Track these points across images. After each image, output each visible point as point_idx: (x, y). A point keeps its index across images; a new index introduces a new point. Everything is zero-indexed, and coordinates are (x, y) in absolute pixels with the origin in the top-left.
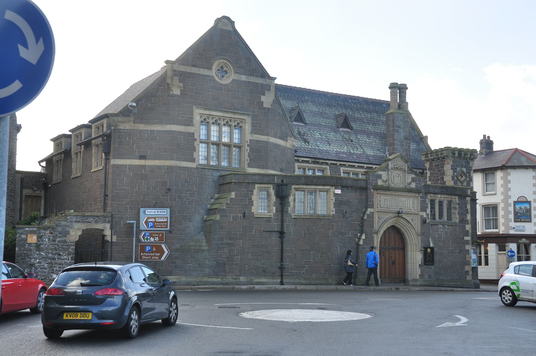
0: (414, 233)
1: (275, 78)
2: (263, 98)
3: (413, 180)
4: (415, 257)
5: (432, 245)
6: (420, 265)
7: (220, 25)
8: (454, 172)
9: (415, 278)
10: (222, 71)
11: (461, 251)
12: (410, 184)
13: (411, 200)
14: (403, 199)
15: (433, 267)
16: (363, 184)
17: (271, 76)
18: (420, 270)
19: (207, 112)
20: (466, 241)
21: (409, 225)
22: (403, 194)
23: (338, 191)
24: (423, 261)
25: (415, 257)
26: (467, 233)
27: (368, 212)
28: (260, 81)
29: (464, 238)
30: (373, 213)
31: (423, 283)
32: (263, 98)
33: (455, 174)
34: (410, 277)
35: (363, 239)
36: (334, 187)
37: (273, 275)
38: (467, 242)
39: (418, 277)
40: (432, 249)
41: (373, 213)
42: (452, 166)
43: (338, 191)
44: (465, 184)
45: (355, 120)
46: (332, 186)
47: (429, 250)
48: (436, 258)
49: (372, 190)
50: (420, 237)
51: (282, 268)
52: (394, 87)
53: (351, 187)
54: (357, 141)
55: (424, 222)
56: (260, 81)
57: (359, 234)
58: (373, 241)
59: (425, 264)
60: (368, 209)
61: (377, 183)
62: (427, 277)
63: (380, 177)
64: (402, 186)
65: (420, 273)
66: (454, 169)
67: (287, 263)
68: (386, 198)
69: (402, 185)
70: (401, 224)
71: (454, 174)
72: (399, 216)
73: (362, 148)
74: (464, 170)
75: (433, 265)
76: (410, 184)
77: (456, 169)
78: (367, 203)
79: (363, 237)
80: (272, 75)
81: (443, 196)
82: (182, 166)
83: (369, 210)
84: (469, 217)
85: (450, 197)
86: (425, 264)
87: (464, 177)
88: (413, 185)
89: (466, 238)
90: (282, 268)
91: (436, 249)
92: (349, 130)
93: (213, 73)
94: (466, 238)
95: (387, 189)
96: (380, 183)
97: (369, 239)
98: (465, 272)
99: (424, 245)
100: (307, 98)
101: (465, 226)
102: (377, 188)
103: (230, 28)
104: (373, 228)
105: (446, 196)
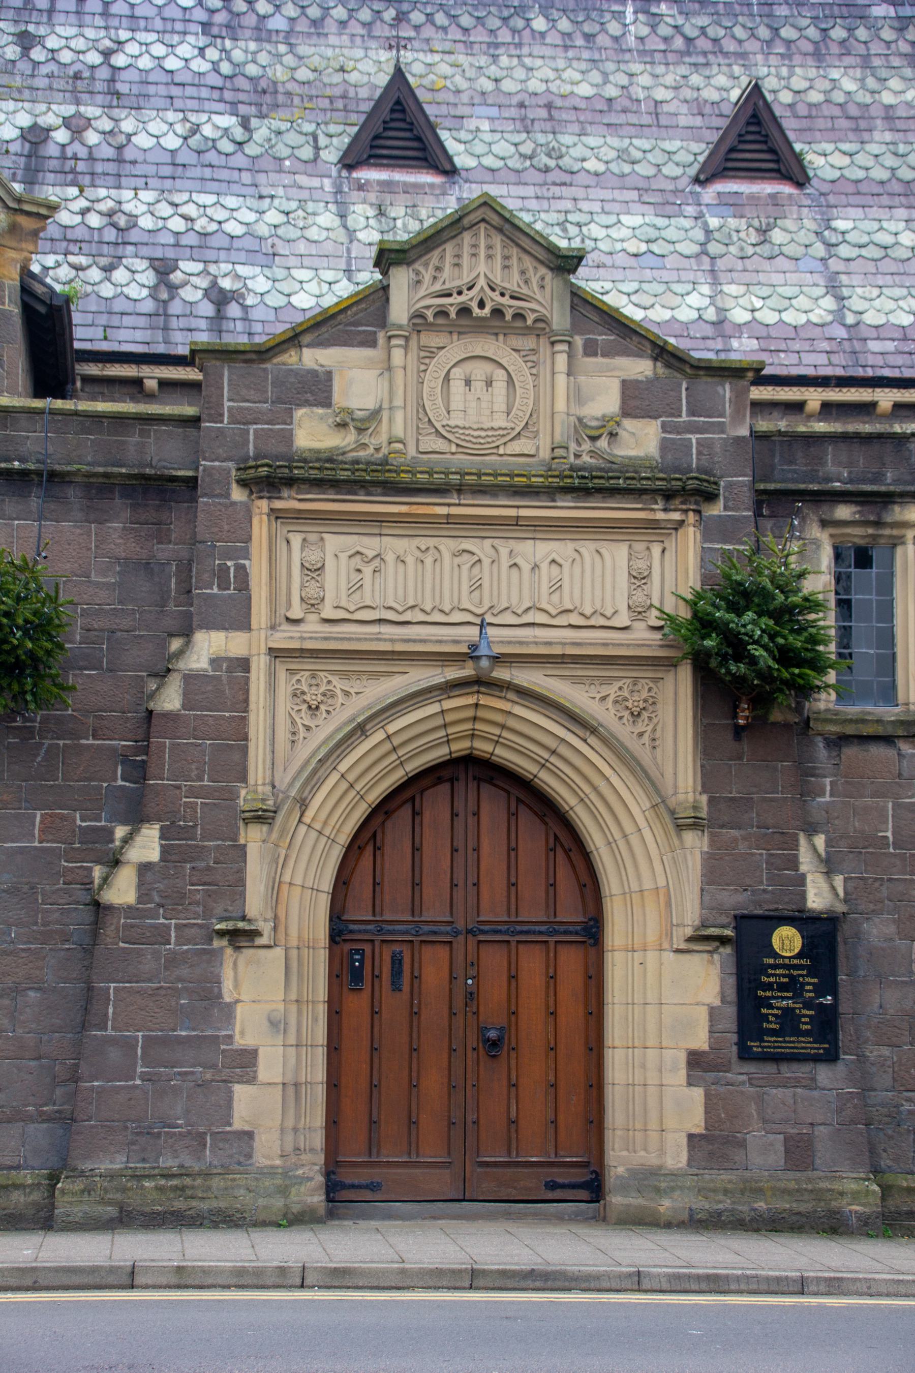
0: (637, 803)
4: (662, 997)
5: (818, 896)
6: (695, 1060)
9: (652, 1160)
13: (622, 551)
14: (543, 550)
15: (824, 1074)
16: (165, 454)
21: (592, 752)
24: (729, 1022)
25: (662, 997)
30: (244, 664)
34: (619, 1159)
35: (144, 868)
39: (676, 1157)
40: (822, 933)
41: (244, 664)
47: (787, 940)
49: (238, 495)
50: (696, 844)
54: (819, 250)
57: (120, 832)
58: (240, 882)
59: (745, 1055)
60: (200, 637)
61: (288, 437)
62: (777, 1157)
63: (317, 389)
64: (535, 449)
65: (696, 1122)
68: (370, 545)
69: (523, 446)
70: (523, 739)
72: (480, 683)
73: (833, 287)
75: (831, 1057)
78: (200, 590)
83: (207, 647)
86: (745, 1055)
88: (642, 441)
91: (877, 930)
92: (787, 189)
95: (368, 485)
96: (311, 433)
97: (203, 873)
99: (736, 899)
100: (540, 24)
102: (275, 477)
104: (244, 779)
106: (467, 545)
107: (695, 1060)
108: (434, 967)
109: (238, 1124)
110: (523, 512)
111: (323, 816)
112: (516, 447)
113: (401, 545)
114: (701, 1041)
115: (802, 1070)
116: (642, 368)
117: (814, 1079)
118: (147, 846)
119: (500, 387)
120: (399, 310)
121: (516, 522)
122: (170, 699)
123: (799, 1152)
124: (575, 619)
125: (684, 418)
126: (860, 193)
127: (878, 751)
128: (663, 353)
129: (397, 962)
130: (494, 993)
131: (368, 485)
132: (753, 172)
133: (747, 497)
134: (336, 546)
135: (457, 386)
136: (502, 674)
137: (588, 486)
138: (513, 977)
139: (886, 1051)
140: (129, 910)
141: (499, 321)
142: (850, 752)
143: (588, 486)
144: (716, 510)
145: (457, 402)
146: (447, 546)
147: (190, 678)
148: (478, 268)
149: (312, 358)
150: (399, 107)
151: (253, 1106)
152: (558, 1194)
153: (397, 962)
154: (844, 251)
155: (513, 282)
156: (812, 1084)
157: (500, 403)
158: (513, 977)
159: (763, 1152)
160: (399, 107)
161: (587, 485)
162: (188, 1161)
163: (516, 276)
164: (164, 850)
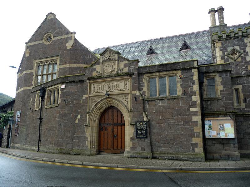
1: (74, 33)
2: (67, 45)
3: (125, 66)
5: (145, 119)
6: (131, 139)
7: (48, 18)
8: (224, 52)
10: (49, 38)
11: (185, 123)
12: (123, 69)
14: (115, 83)
15: (146, 140)
17: (71, 31)
18: (131, 143)
19: (40, 61)
20: (193, 112)
22: (114, 79)
23: (63, 87)
24: (135, 134)
26: (194, 104)
27: (84, 98)
28: (66, 36)
29: (189, 110)
31: (134, 155)
32: (67, 45)
33: (226, 53)
35: (79, 119)
36: (61, 84)
37: (34, 145)
38: (195, 114)
42: (221, 47)
43: (63, 87)
44: (240, 59)
45: (192, 44)
46: (60, 83)
48: (155, 131)
51: (40, 141)
52: (212, 11)
53: (74, 82)
55: (135, 99)
56: (66, 36)
63: (95, 70)
64: (115, 73)
65: (131, 145)
66: (223, 49)
67: (42, 139)
69: (114, 72)
70: (115, 103)
71: (224, 54)
74: (238, 48)
75: (146, 138)
76: (123, 69)
77: (227, 49)
79: (79, 117)
80: (71, 31)
81: (162, 73)
82: (27, 89)
84: (196, 88)
85: (171, 72)
86: (137, 138)
87: (238, 54)
88: (126, 70)
89: (192, 110)
90: (40, 141)
91: (153, 123)
93: (44, 41)
94: (192, 110)
95: (98, 78)
96: (94, 74)
98: (193, 144)
99: (135, 120)
101: (191, 98)
103: (52, 17)
105: (165, 73)
106: (108, 83)
107: (131, 139)
108: (110, 128)
109: (86, 145)
110: (113, 79)
111: (95, 113)
112: (113, 72)
113: (102, 84)
114: (132, 136)
115: (143, 139)
116: (126, 62)
117: (144, 140)
118: (79, 117)
119: (111, 67)
120: (101, 61)
121: (113, 80)
122: (81, 102)
123: (143, 149)
124: (119, 90)
125: (130, 67)
126: (196, 49)
127: (154, 102)
128: (128, 60)
129: (106, 128)
130: (115, 131)
131: (98, 78)
132: (186, 49)
133: (137, 74)
134: (96, 85)
135: (107, 67)
136: (111, 97)
137: (119, 76)
138: (117, 129)
139: (154, 137)
140: (78, 123)
141: (110, 60)
142: (150, 102)
143: (119, 76)
144: (133, 76)
145: (107, 69)
146: (106, 84)
147: (83, 100)
148: (107, 55)
149: (94, 67)
150: (151, 49)
151: (88, 143)
152: (122, 153)
153: (106, 128)
154: (194, 54)
155: (112, 56)
156: (144, 141)
157: (111, 68)
158: (117, 129)
159: (139, 149)
160: (151, 49)
161: (118, 75)
162: (82, 148)
163: (112, 55)
164: (80, 117)
